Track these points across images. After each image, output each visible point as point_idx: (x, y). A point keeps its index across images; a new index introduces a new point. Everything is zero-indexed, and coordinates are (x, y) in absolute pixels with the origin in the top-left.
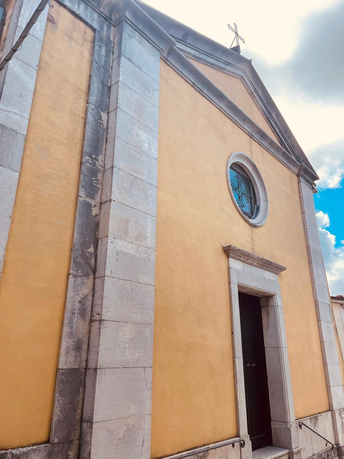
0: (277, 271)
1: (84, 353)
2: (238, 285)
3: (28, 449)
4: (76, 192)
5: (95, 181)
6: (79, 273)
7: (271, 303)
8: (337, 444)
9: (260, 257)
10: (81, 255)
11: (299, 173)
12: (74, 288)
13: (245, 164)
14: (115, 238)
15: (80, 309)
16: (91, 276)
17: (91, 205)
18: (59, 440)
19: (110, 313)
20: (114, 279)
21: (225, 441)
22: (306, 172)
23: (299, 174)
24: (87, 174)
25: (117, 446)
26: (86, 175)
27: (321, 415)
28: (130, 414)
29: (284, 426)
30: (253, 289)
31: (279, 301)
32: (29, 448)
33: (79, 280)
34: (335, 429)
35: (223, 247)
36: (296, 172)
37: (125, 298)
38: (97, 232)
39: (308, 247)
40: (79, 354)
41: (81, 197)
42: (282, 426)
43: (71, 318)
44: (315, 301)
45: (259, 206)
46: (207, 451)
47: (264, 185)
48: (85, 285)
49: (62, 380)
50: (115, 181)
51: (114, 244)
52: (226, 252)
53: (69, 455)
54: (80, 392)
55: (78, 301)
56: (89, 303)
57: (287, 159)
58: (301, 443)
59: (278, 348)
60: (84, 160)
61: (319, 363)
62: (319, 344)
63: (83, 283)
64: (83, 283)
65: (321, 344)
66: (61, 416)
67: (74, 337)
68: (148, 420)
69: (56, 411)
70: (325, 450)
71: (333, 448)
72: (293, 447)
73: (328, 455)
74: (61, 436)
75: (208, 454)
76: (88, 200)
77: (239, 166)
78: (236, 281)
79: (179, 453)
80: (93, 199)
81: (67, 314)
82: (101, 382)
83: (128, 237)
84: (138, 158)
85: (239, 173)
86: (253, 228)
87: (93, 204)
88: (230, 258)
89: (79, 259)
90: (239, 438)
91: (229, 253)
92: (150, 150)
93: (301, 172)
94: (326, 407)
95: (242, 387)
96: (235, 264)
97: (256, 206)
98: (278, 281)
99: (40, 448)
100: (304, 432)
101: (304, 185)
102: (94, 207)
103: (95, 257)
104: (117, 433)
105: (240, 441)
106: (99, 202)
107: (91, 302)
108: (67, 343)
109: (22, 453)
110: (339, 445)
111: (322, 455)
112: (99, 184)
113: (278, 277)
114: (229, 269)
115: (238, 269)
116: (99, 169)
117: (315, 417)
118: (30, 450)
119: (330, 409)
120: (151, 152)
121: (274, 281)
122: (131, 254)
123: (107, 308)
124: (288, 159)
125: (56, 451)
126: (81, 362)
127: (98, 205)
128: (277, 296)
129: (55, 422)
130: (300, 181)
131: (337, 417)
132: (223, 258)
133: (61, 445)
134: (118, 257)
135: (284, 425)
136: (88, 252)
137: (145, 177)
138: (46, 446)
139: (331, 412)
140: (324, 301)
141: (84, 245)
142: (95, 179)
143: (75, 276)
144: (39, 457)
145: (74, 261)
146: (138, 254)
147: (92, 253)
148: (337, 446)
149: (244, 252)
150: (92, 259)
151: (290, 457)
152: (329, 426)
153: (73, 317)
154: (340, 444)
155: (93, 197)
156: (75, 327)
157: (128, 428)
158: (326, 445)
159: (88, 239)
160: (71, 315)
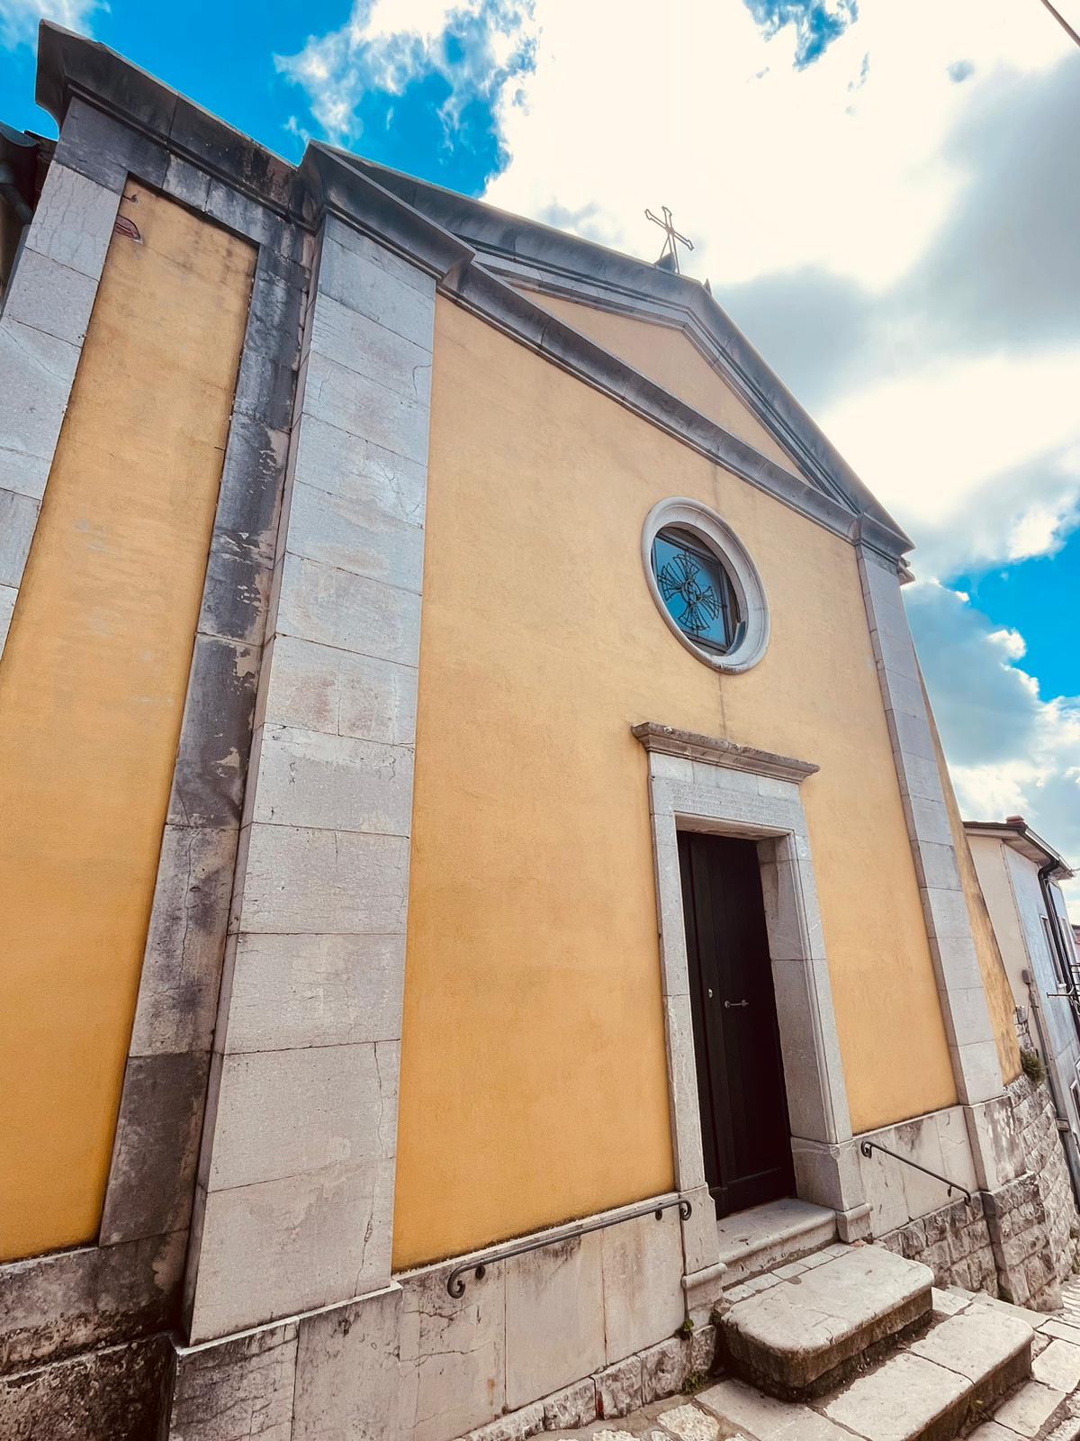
0: (794, 774)
1: (205, 1014)
2: (676, 817)
3: (29, 1266)
4: (194, 624)
5: (246, 594)
6: (193, 818)
7: (780, 852)
8: (982, 1189)
9: (739, 746)
10: (200, 776)
11: (858, 537)
12: (179, 857)
13: (701, 525)
14: (285, 727)
15: (194, 907)
16: (229, 824)
17: (233, 651)
18: (125, 1235)
19: (267, 913)
20: (280, 828)
21: (635, 1206)
22: (876, 533)
23: (859, 540)
24: (222, 578)
25: (285, 1248)
26: (219, 580)
27: (931, 1117)
28: (328, 1163)
29: (821, 1152)
30: (724, 823)
31: (801, 848)
32: (32, 1263)
33: (194, 837)
34: (974, 1149)
35: (632, 728)
36: (851, 536)
37: (314, 875)
38: (252, 716)
39: (888, 713)
40: (190, 1017)
41: (205, 633)
42: (816, 1151)
43: (168, 930)
44: (910, 841)
45: (744, 622)
46: (577, 1235)
47: (755, 572)
48: (210, 847)
49: (137, 1086)
50: (290, 588)
51: (280, 743)
52: (641, 739)
53: (157, 1272)
54: (195, 1110)
55: (190, 887)
56: (223, 891)
57: (819, 506)
58: (869, 1192)
59: (800, 960)
60: (214, 546)
61: (925, 989)
62: (925, 940)
63: (205, 842)
64: (205, 842)
65: (929, 943)
66: (133, 1175)
67: (178, 978)
68: (385, 1176)
69: (117, 1164)
70: (946, 1207)
71: (967, 1201)
72: (846, 1205)
73: (953, 1221)
74: (132, 1225)
75: (579, 1244)
76: (225, 640)
77: (686, 532)
78: (670, 808)
79: (492, 1244)
80: (241, 636)
81: (157, 923)
82: (235, 1088)
83: (326, 722)
84: (362, 528)
85: (687, 549)
86: (724, 678)
87: (240, 649)
88: (651, 753)
89: (195, 786)
90: (676, 1194)
91: (648, 742)
92: (402, 507)
93: (863, 536)
94: (948, 1095)
95: (687, 1068)
96: (666, 767)
97: (738, 625)
98: (798, 799)
99: (65, 1261)
100: (880, 1163)
101: (871, 564)
102: (242, 656)
103: (242, 778)
104: (286, 1213)
105: (679, 1204)
106: (258, 642)
107: (228, 888)
108: (155, 992)
109: (9, 1277)
110: (988, 1191)
111: (936, 1220)
112: (260, 600)
113: (800, 790)
114: (650, 779)
115: (678, 778)
116: (259, 565)
117: (912, 1126)
118: (33, 1269)
119: (960, 1100)
120: (404, 511)
121: (786, 800)
122: (335, 764)
123: (256, 903)
124: (823, 505)
125: (113, 1264)
126: (196, 1037)
127: (255, 650)
128: (796, 837)
129: (115, 1190)
130: (862, 557)
131: (980, 1120)
132: (634, 754)
133: (131, 1249)
134: (293, 774)
135: (820, 1149)
136: (221, 766)
137: (385, 573)
138: (84, 1253)
139: (961, 1107)
140: (936, 836)
141: (210, 751)
142: (246, 588)
143: (181, 828)
144: (60, 1285)
145: (179, 792)
146: (358, 761)
147: (233, 767)
148: (982, 1194)
149: (690, 735)
150: (232, 784)
151: (840, 1230)
152: (955, 1145)
153: (175, 928)
154: (990, 1188)
155: (240, 632)
156: (179, 952)
157: (319, 1198)
158: (949, 1192)
159: (221, 735)
160: (168, 924)
